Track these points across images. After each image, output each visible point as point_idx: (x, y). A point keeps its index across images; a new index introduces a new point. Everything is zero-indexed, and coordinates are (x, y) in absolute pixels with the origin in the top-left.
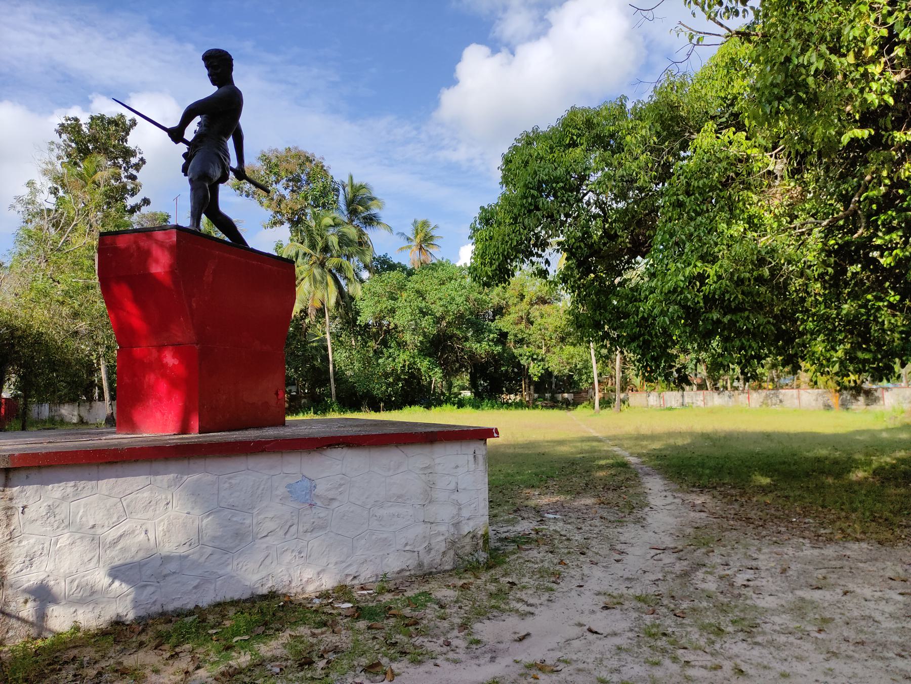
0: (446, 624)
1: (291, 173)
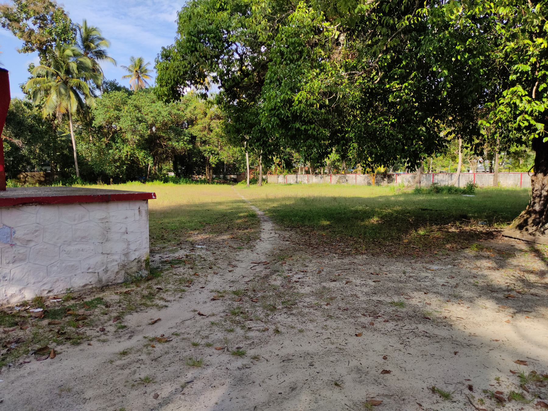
0: (106, 317)
1: (38, 13)
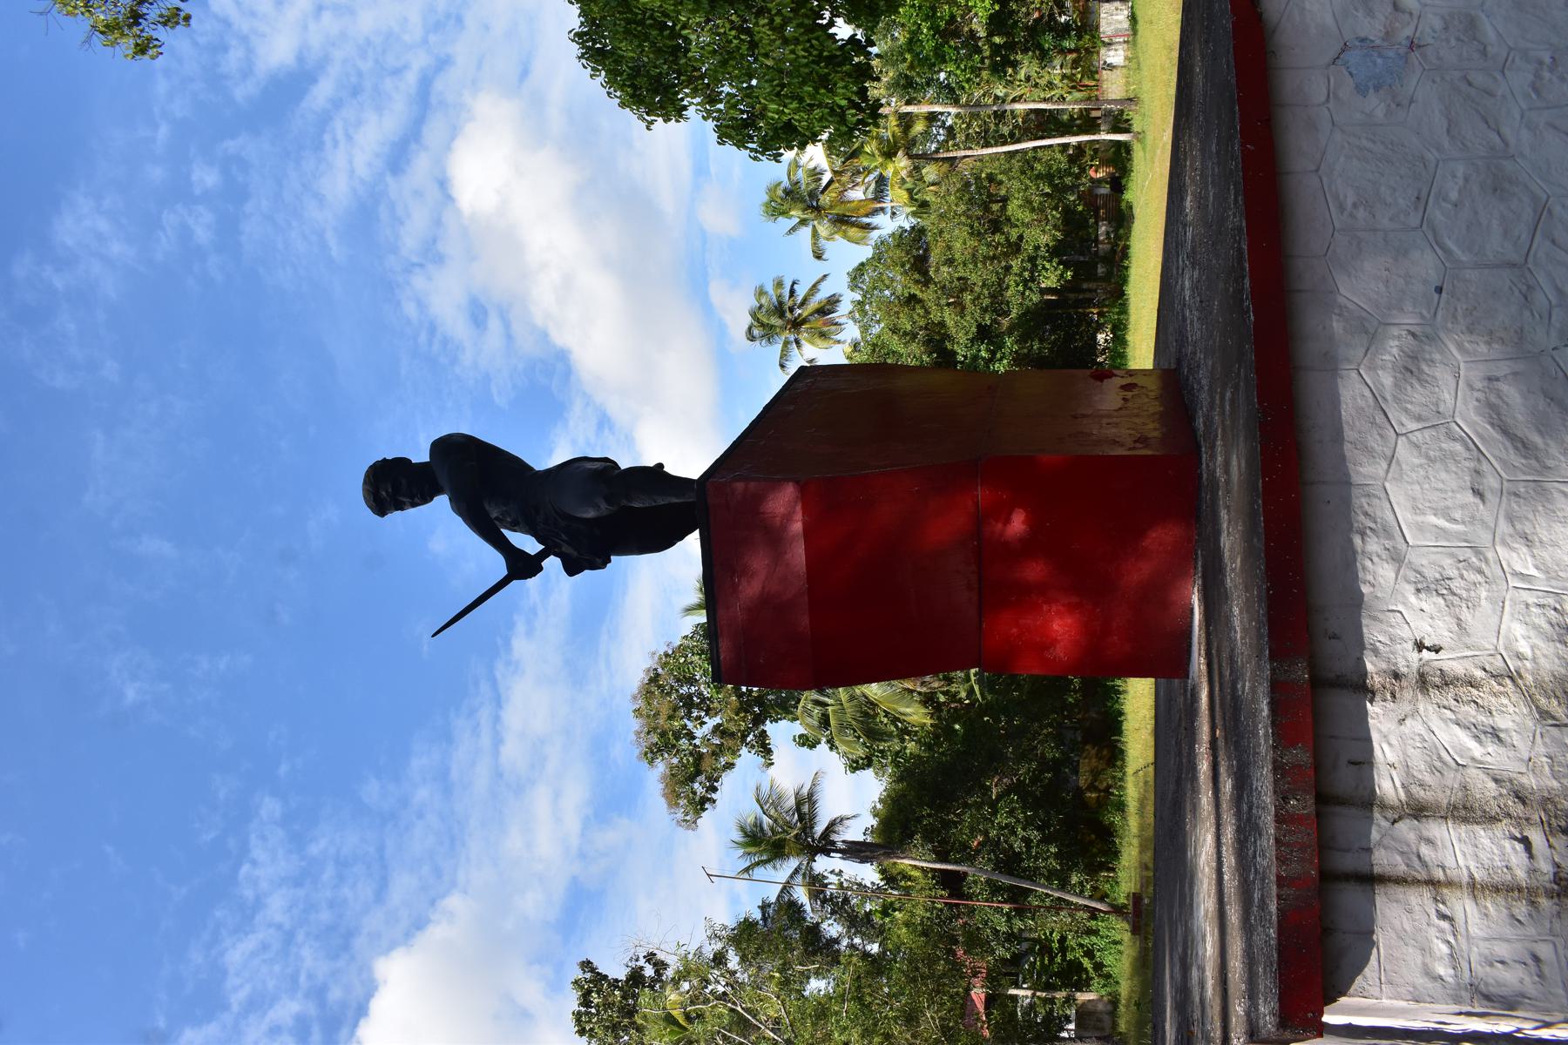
1: (675, 709)
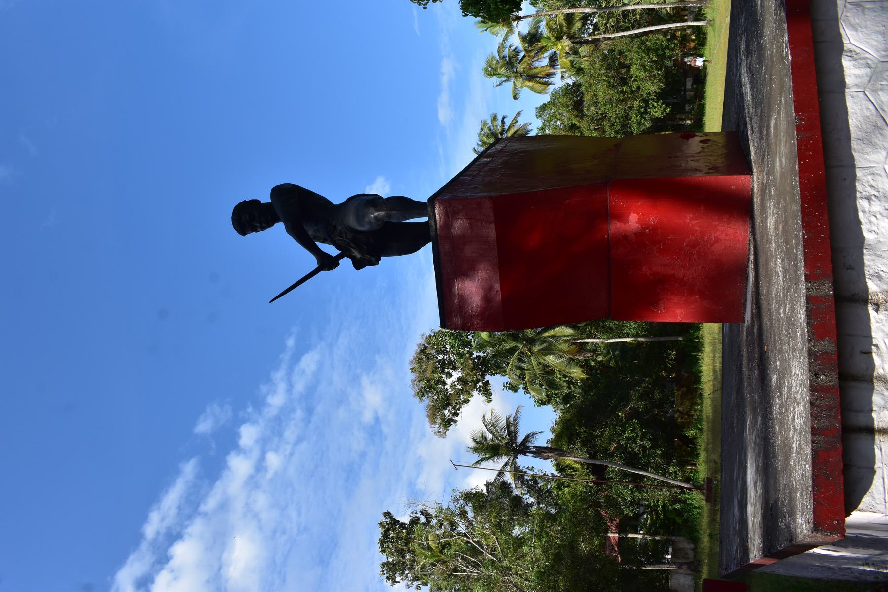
1: (436, 368)
